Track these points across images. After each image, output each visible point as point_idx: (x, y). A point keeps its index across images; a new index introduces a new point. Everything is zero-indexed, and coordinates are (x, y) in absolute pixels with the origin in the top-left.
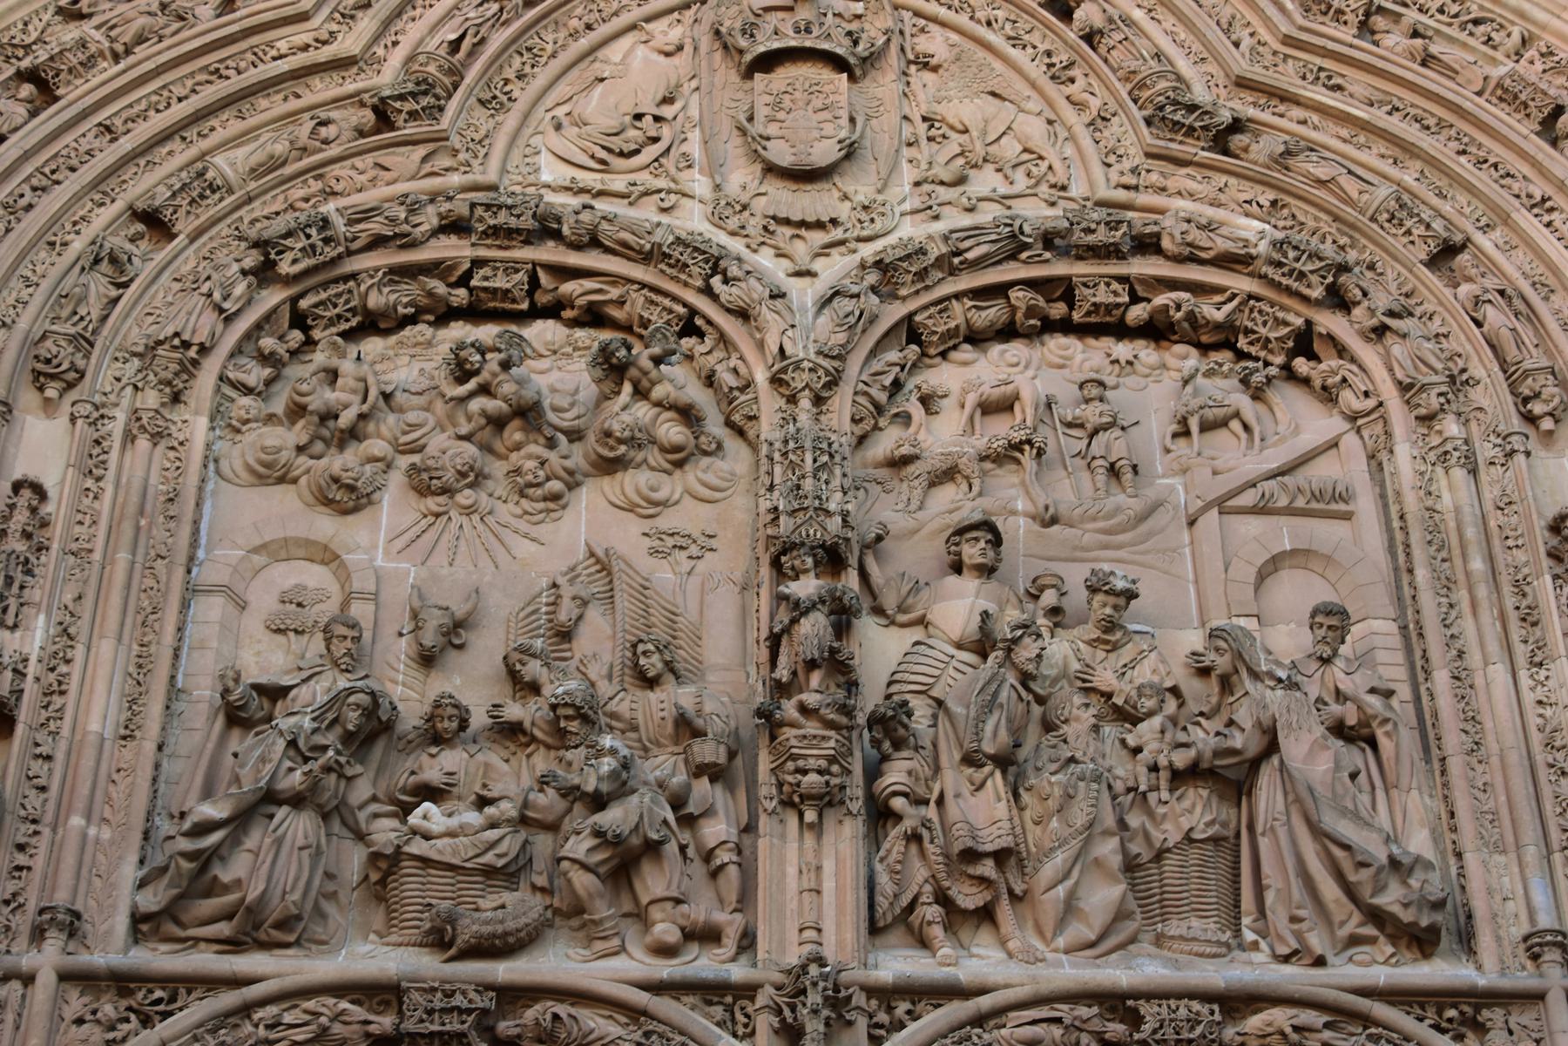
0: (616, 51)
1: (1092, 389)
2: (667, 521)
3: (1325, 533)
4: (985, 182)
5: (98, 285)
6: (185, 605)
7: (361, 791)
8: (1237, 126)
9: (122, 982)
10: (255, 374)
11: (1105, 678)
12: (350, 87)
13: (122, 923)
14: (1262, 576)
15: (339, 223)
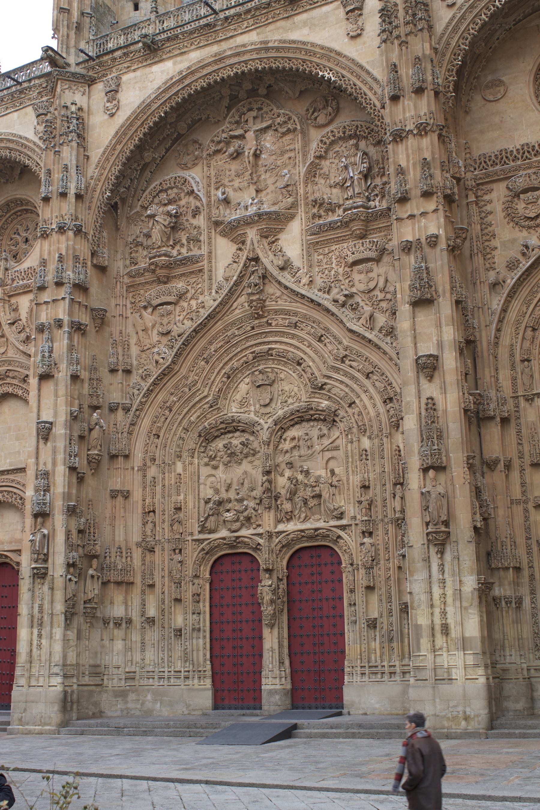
0: (240, 386)
1: (307, 434)
2: (254, 464)
3: (335, 453)
4: (290, 401)
5: (181, 442)
6: (199, 487)
7: (221, 510)
8: (322, 385)
9: (198, 540)
10: (202, 449)
11: (306, 482)
12: (207, 400)
13: (197, 532)
14: (327, 462)
15: (208, 427)
